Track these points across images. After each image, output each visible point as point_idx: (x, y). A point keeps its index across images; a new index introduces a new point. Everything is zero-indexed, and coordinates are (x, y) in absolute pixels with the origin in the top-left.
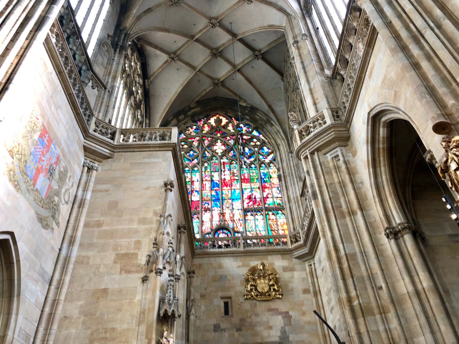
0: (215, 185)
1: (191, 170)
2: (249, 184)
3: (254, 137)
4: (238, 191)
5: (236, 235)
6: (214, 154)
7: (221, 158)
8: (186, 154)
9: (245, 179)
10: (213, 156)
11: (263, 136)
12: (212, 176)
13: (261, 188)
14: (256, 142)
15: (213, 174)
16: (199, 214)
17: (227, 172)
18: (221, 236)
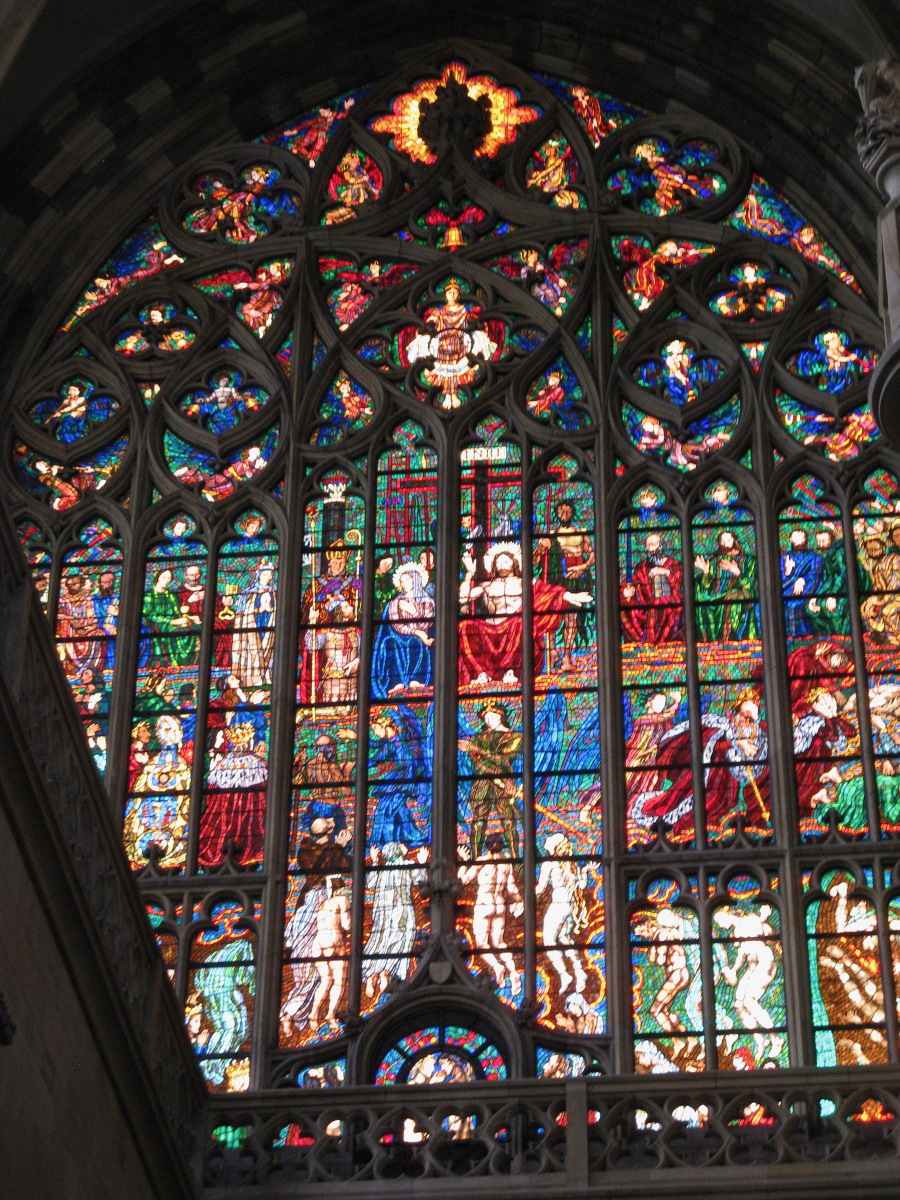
0: (402, 659)
1: (210, 534)
2: (674, 652)
3: (741, 248)
4: (584, 710)
5: (550, 1064)
6: (403, 393)
7: (462, 429)
8: (178, 402)
9: (645, 602)
10: (391, 416)
11: (820, 237)
12: (376, 588)
13: (771, 680)
14: (759, 291)
15: (385, 564)
16: (255, 896)
17: (505, 554)
18: (428, 1071)
